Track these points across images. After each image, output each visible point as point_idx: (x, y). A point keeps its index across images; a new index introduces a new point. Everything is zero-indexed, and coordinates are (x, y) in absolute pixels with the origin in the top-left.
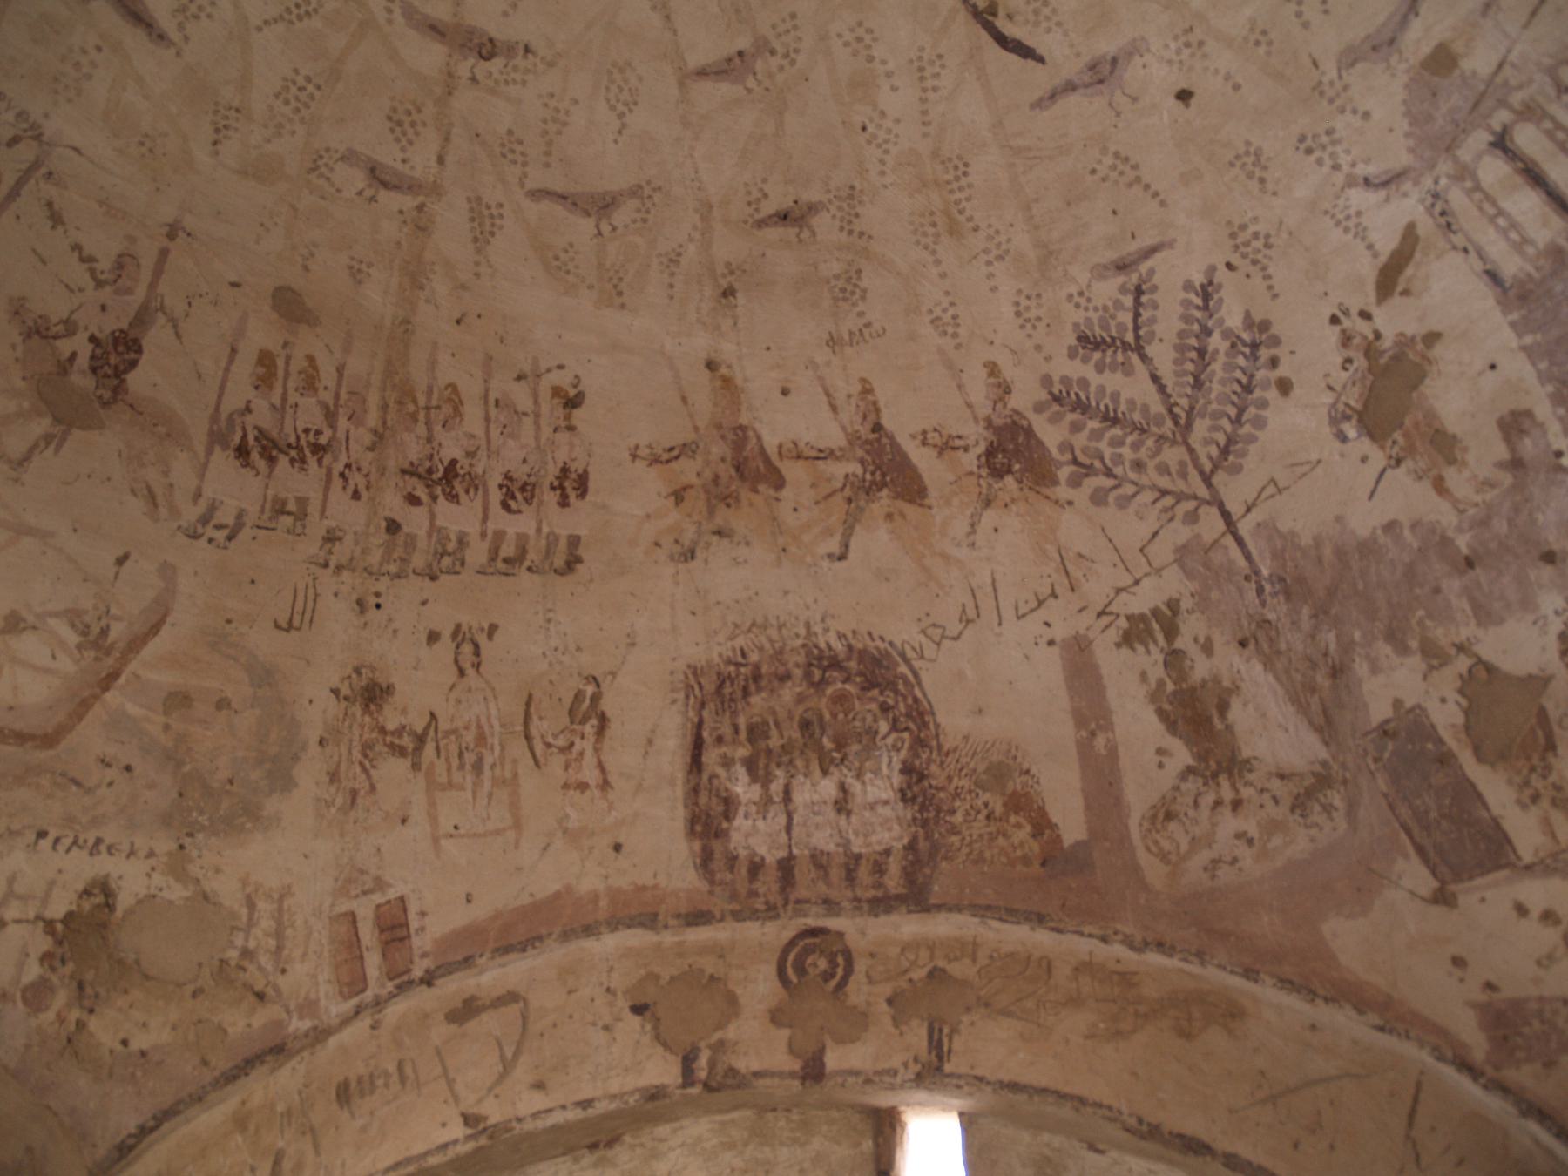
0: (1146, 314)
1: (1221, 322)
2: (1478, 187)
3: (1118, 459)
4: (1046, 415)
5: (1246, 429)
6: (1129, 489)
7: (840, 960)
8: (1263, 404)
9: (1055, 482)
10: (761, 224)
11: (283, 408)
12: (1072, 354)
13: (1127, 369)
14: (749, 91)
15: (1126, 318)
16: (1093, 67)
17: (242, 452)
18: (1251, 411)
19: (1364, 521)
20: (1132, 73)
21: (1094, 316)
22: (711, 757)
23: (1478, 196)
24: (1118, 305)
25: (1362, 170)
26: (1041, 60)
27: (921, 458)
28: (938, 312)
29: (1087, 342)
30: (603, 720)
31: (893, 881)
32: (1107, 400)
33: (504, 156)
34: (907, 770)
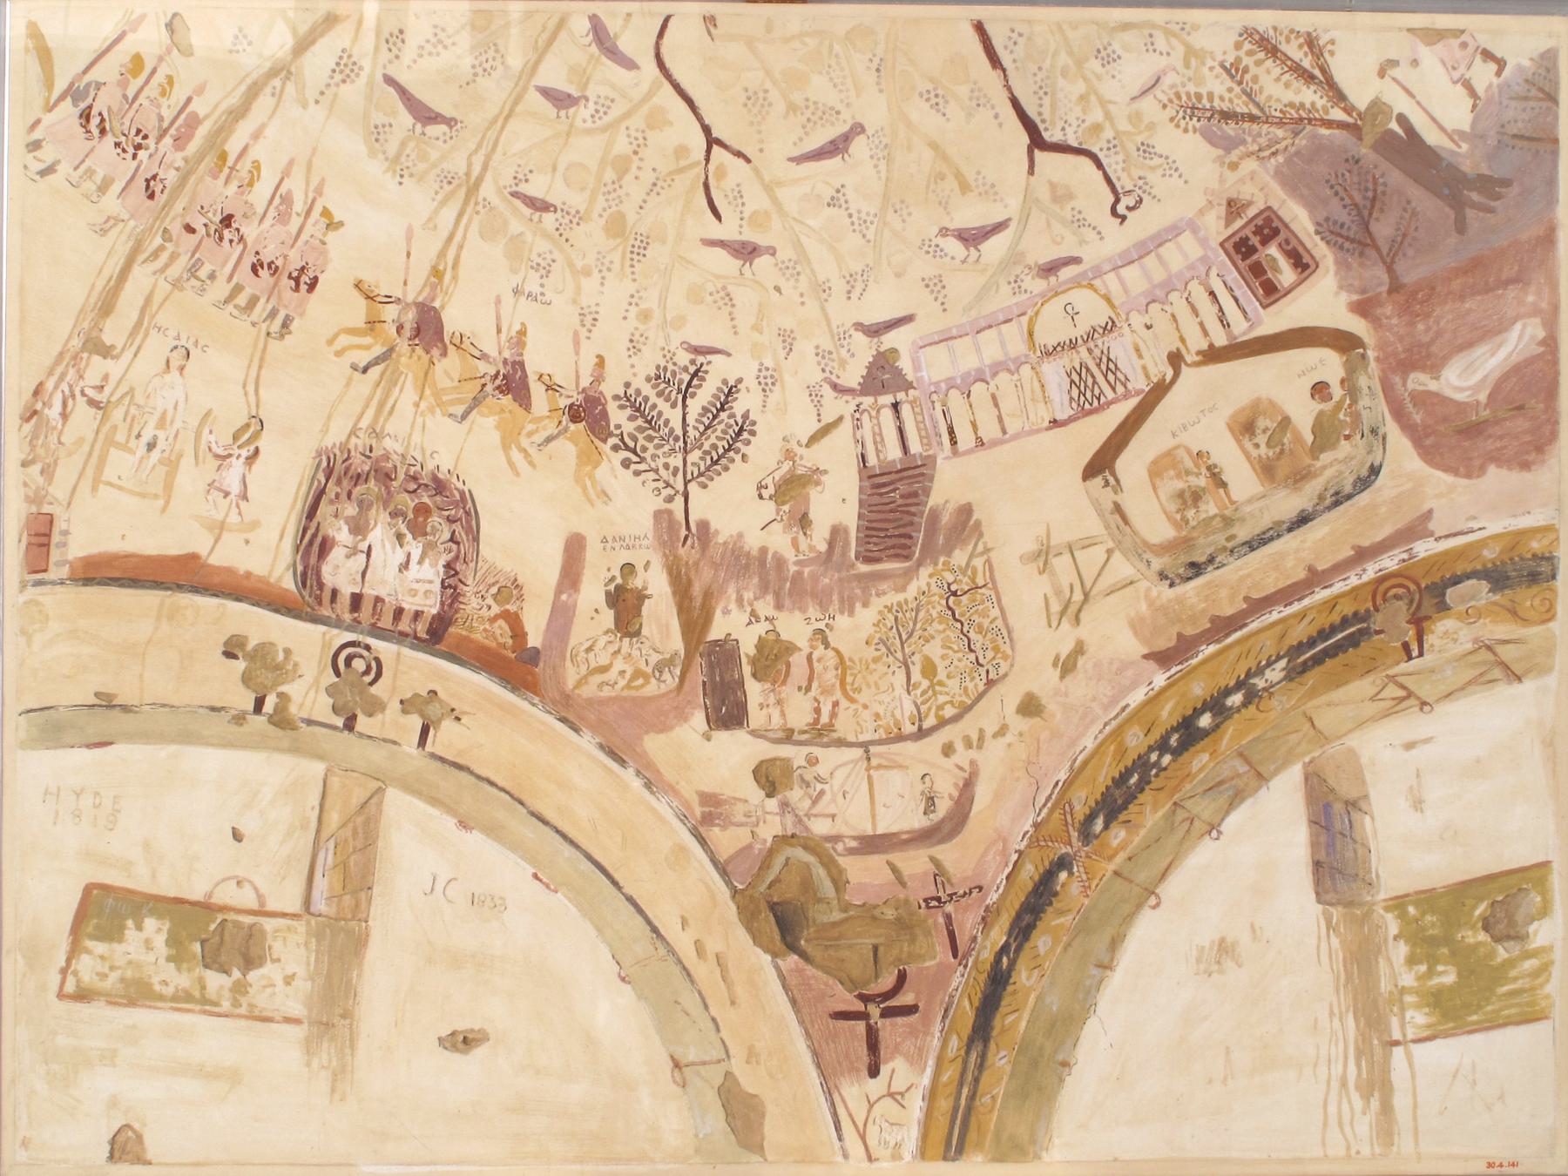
0: (695, 382)
1: (732, 408)
2: (877, 418)
3: (645, 449)
4: (618, 403)
5: (718, 467)
6: (643, 467)
7: (374, 664)
8: (733, 461)
9: (605, 441)
10: (515, 195)
11: (133, 102)
12: (648, 379)
13: (674, 406)
14: (558, 117)
15: (686, 378)
16: (744, 244)
17: (86, 116)
18: (724, 461)
19: (753, 542)
20: (763, 262)
21: (670, 367)
22: (325, 509)
23: (875, 421)
24: (686, 369)
25: (834, 378)
26: (720, 220)
27: (537, 391)
28: (586, 311)
29: (657, 378)
30: (257, 451)
31: (421, 629)
32: (655, 413)
33: (387, 42)
34: (448, 566)
